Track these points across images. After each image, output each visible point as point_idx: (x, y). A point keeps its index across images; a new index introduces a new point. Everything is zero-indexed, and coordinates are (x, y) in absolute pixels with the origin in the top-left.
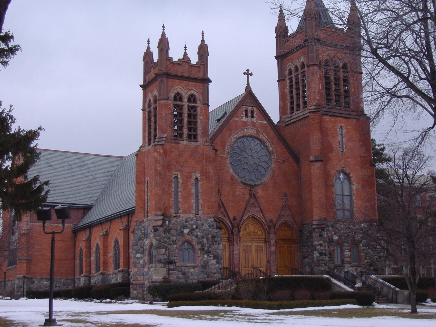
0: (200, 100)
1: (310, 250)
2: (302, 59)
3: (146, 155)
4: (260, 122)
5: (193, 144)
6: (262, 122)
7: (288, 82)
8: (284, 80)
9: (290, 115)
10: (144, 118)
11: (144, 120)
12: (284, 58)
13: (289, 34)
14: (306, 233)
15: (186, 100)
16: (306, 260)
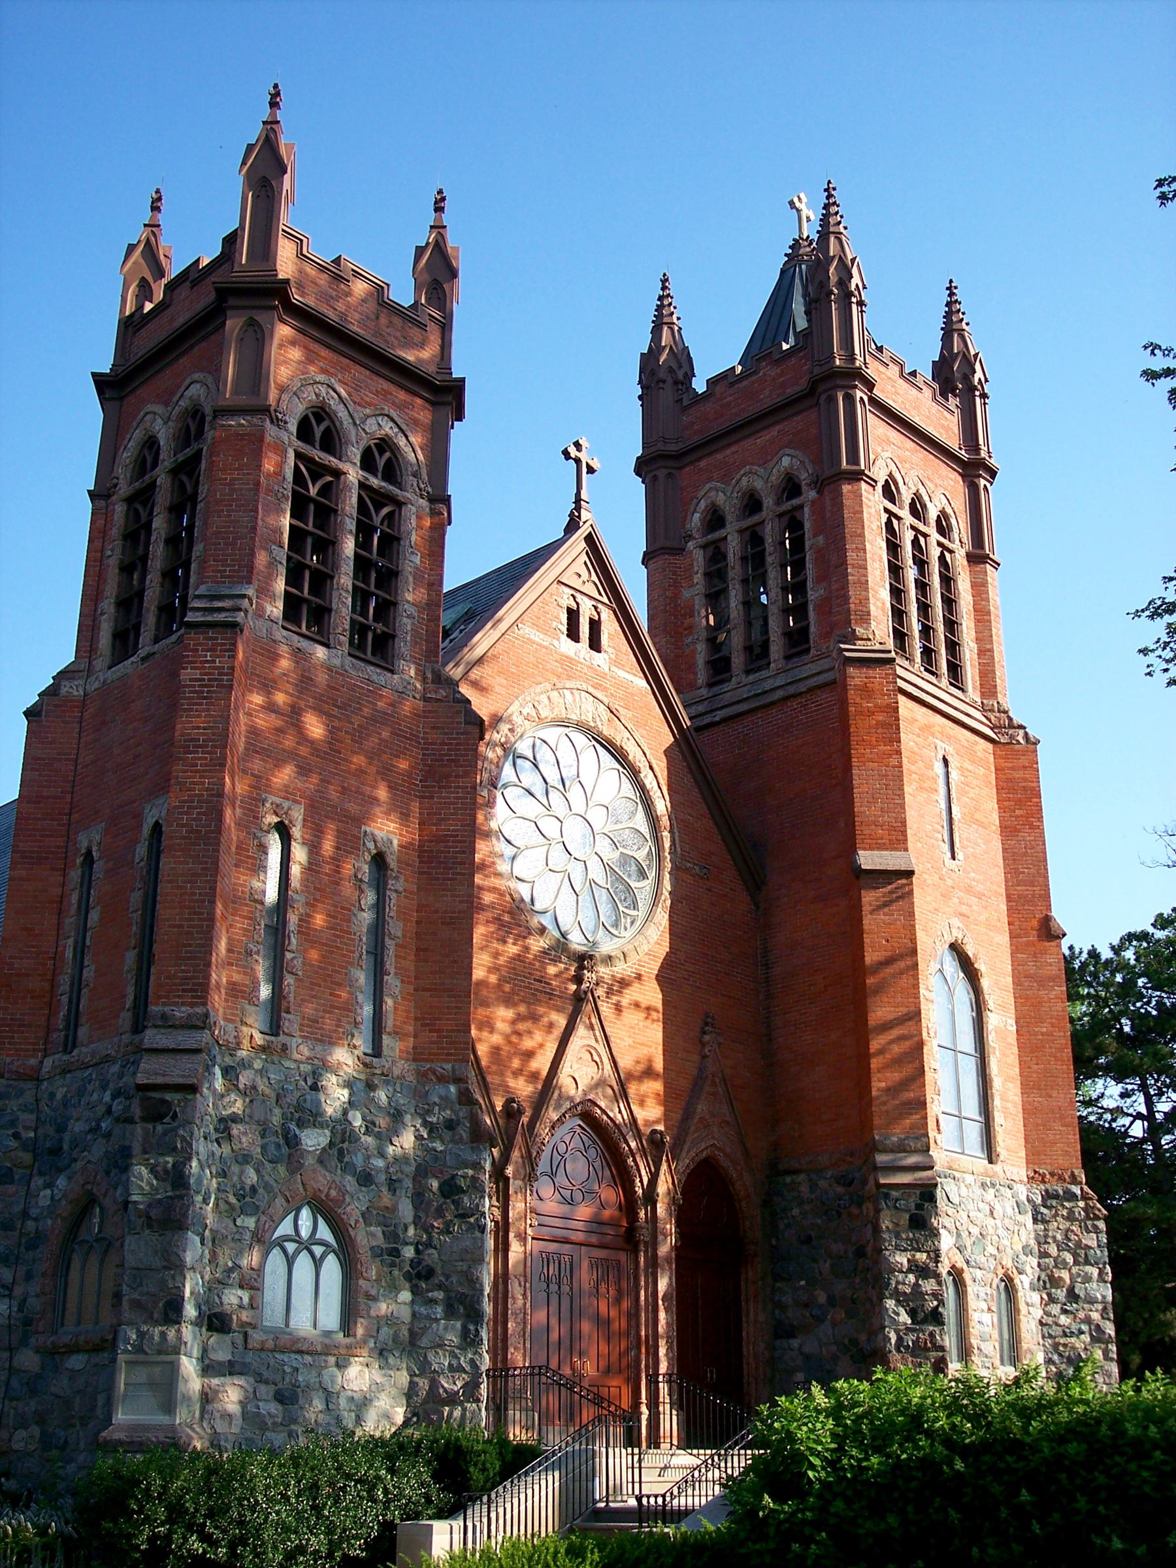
0: (416, 475)
1: (822, 1298)
2: (786, 461)
3: (86, 715)
4: (622, 674)
5: (375, 678)
6: (630, 677)
7: (698, 558)
8: (680, 551)
9: (704, 692)
10: (98, 535)
11: (97, 543)
12: (680, 468)
13: (699, 385)
14: (796, 1212)
15: (355, 453)
16: (795, 1343)
